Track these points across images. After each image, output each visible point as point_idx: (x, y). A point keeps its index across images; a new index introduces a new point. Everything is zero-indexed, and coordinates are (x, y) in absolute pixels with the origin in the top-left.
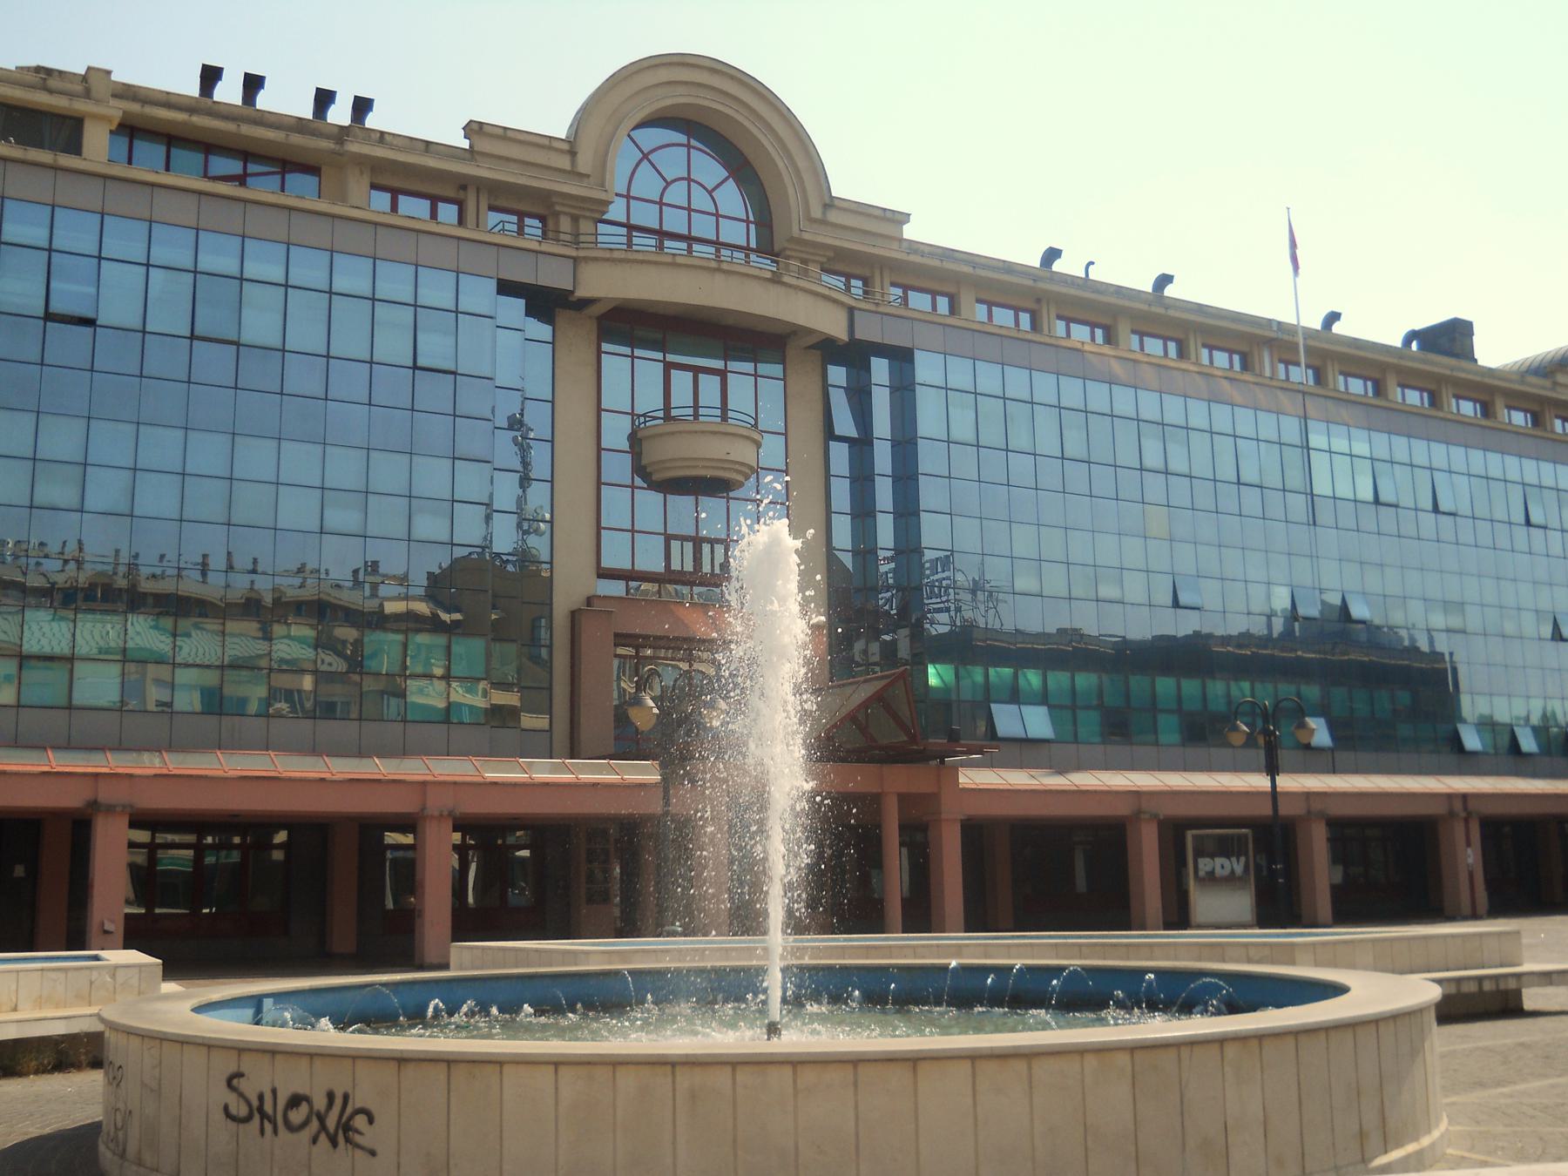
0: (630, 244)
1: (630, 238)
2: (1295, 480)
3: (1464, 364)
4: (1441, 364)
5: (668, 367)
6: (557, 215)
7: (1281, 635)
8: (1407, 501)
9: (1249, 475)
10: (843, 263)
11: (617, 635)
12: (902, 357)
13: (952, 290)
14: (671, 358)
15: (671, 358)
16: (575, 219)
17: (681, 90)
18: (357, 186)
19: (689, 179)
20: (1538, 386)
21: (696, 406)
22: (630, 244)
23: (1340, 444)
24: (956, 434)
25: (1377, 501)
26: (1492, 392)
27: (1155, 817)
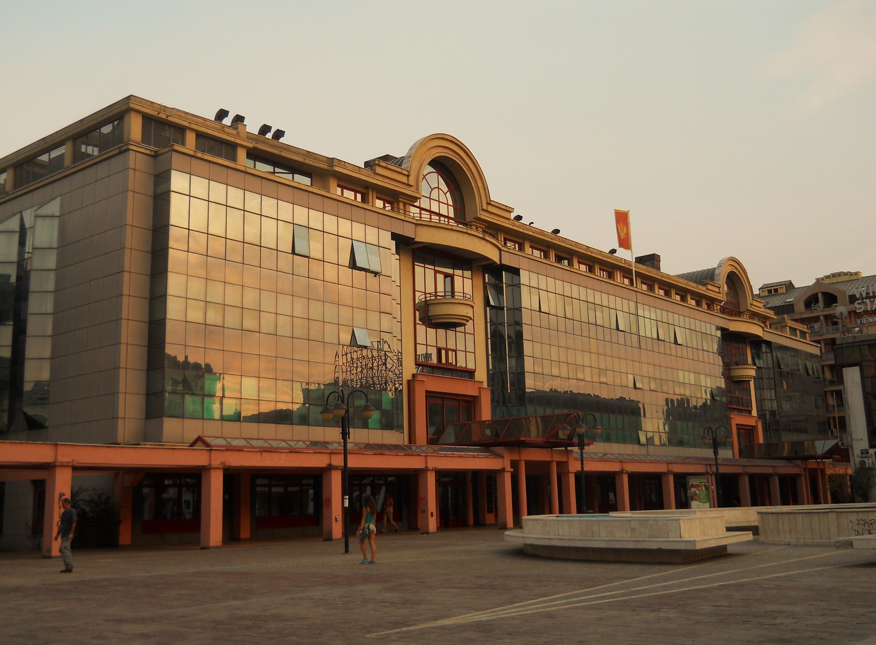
0: (431, 218)
1: (421, 214)
2: (634, 330)
3: (654, 271)
4: (643, 269)
5: (436, 272)
6: (398, 202)
7: (701, 407)
8: (667, 340)
9: (569, 315)
10: (492, 230)
11: (427, 392)
12: (516, 271)
13: (521, 241)
14: (437, 268)
15: (437, 268)
16: (405, 204)
17: (441, 150)
18: (333, 184)
19: (438, 188)
20: (683, 283)
21: (445, 292)
22: (431, 218)
23: (647, 315)
24: (591, 321)
25: (658, 339)
26: (669, 287)
27: (627, 472)
